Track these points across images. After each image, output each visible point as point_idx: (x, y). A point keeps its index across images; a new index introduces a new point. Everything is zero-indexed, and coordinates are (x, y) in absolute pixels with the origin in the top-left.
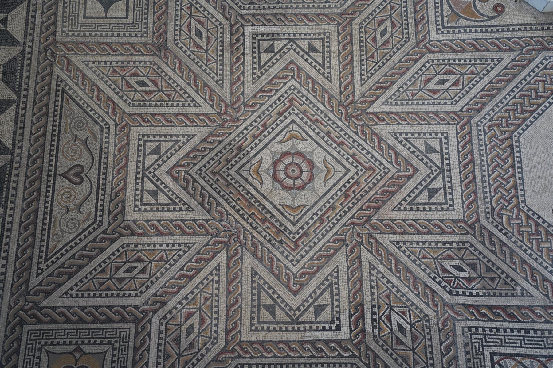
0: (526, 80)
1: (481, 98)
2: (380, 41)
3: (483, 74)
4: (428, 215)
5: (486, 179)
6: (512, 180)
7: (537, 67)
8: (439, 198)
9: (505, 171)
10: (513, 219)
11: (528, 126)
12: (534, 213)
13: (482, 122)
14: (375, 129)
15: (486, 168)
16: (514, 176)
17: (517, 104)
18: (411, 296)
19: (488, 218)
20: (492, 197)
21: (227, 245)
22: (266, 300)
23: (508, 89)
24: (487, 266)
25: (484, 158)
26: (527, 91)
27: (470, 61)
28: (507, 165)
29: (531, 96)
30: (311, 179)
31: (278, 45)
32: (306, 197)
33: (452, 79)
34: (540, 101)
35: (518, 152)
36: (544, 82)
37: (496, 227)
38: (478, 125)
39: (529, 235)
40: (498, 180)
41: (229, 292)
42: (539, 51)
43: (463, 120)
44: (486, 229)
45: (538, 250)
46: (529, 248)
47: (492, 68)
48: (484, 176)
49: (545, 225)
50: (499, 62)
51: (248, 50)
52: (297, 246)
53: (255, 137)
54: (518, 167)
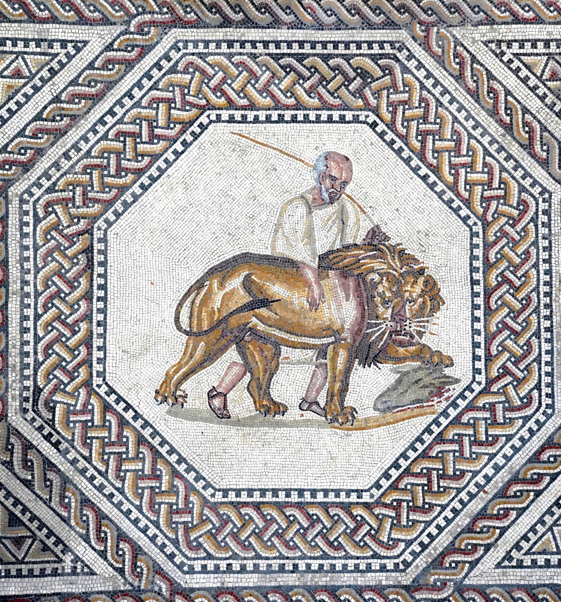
0: (131, 97)
1: (34, 136)
3: (41, 79)
5: (30, 324)
6: (83, 326)
7: (158, 66)
9: (72, 307)
10: (75, 413)
11: (127, 206)
12: (120, 399)
13: (31, 195)
15: (31, 301)
16: (88, 317)
17: (110, 152)
19: (25, 411)
20: (38, 365)
23: (94, 116)
24: (11, 514)
25: (30, 277)
26: (133, 122)
27: (15, 45)
28: (77, 293)
29: (140, 135)
34: (157, 147)
35: (101, 264)
36: (170, 101)
37: (40, 429)
38: (22, 201)
39: (104, 445)
40: (54, 328)
42: (166, 26)
44: (19, 434)
45: (118, 477)
46: (100, 472)
47: (62, 65)
48: (27, 318)
49: (138, 424)
50: (78, 50)
54: (99, 299)
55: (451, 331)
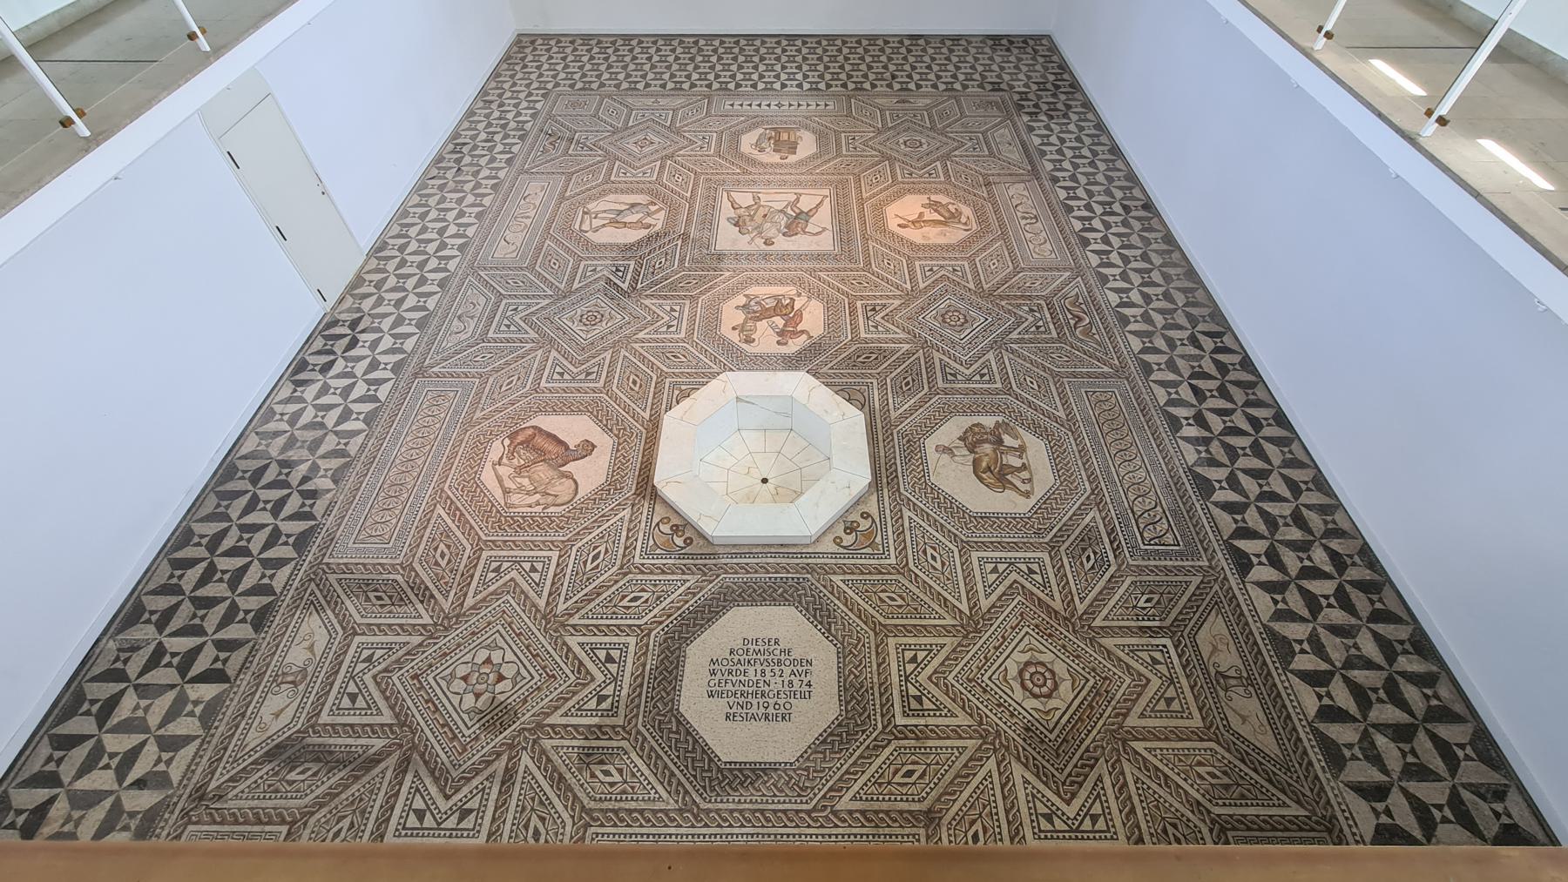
2: (900, 602)
4: (1051, 576)
8: (1035, 567)
14: (984, 610)
18: (1121, 591)
21: (1124, 742)
22: (1162, 705)
30: (1042, 664)
31: (913, 691)
32: (1060, 669)
33: (930, 551)
41: (1167, 739)
43: (965, 547)
51: (922, 721)
52: (1105, 679)
53: (1012, 715)
55: (989, 421)
